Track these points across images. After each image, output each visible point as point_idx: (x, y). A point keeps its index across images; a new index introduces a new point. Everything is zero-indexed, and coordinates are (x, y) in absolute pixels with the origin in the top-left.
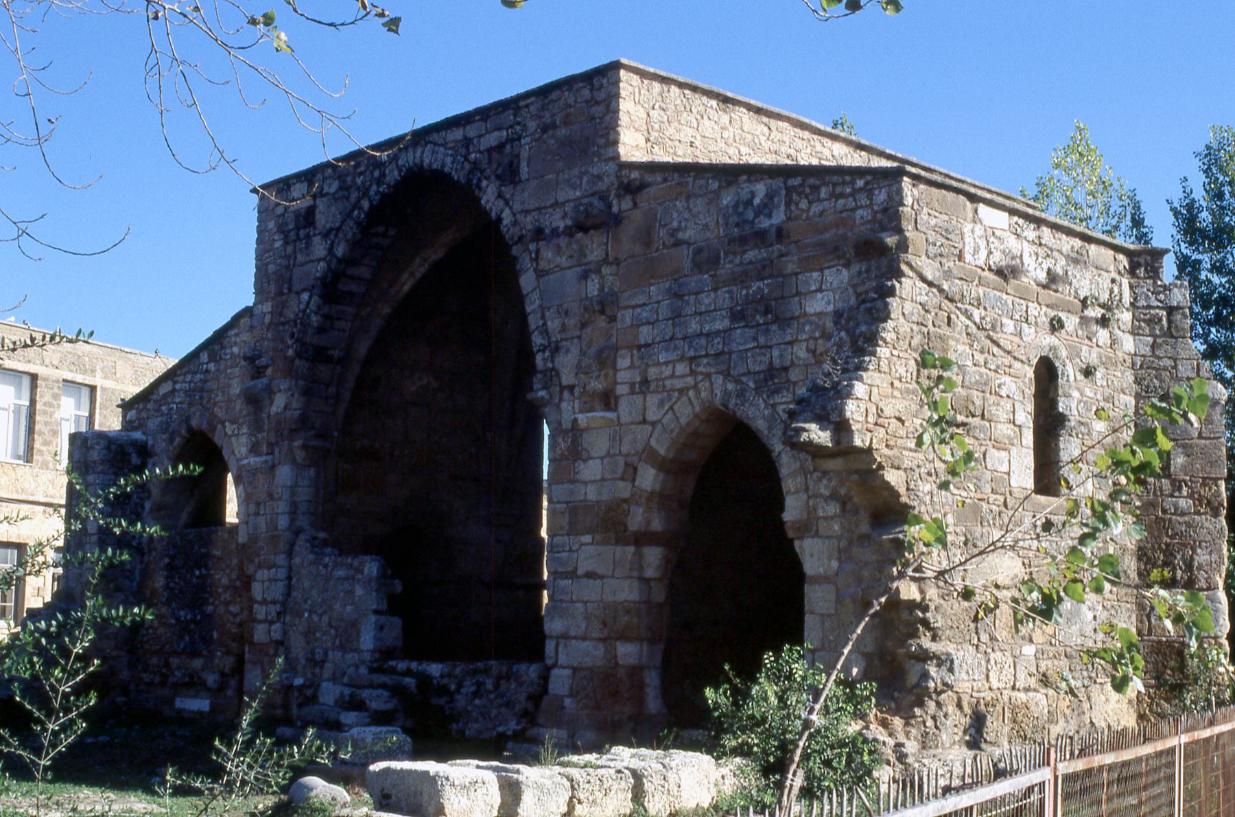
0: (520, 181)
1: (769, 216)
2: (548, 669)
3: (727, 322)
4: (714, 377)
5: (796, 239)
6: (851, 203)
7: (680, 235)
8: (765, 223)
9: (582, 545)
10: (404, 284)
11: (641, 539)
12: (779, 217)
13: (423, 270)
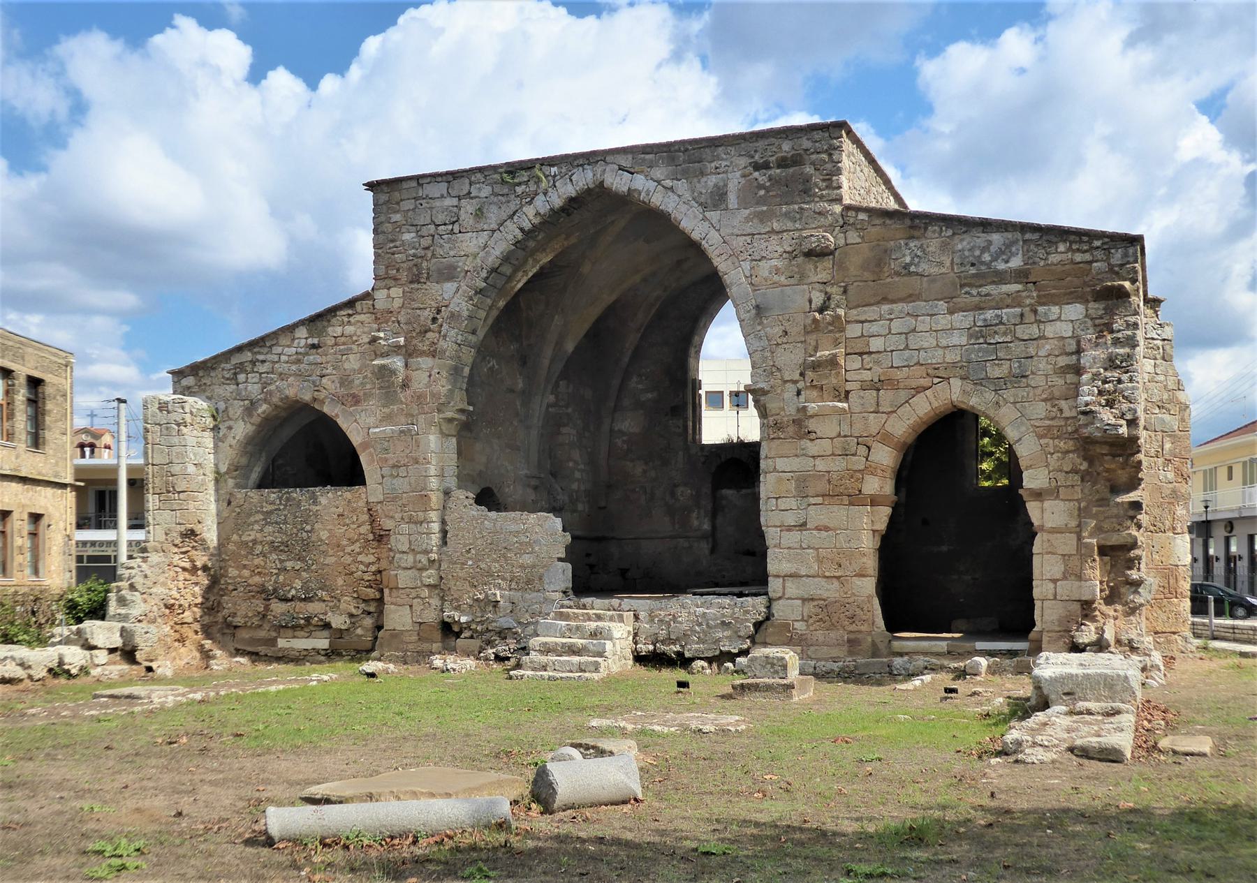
0: (726, 209)
1: (1007, 262)
2: (770, 600)
3: (964, 340)
4: (952, 380)
5: (1034, 280)
6: (1088, 257)
7: (913, 269)
8: (1001, 266)
9: (809, 505)
10: (519, 281)
11: (874, 501)
12: (1016, 262)
13: (534, 270)
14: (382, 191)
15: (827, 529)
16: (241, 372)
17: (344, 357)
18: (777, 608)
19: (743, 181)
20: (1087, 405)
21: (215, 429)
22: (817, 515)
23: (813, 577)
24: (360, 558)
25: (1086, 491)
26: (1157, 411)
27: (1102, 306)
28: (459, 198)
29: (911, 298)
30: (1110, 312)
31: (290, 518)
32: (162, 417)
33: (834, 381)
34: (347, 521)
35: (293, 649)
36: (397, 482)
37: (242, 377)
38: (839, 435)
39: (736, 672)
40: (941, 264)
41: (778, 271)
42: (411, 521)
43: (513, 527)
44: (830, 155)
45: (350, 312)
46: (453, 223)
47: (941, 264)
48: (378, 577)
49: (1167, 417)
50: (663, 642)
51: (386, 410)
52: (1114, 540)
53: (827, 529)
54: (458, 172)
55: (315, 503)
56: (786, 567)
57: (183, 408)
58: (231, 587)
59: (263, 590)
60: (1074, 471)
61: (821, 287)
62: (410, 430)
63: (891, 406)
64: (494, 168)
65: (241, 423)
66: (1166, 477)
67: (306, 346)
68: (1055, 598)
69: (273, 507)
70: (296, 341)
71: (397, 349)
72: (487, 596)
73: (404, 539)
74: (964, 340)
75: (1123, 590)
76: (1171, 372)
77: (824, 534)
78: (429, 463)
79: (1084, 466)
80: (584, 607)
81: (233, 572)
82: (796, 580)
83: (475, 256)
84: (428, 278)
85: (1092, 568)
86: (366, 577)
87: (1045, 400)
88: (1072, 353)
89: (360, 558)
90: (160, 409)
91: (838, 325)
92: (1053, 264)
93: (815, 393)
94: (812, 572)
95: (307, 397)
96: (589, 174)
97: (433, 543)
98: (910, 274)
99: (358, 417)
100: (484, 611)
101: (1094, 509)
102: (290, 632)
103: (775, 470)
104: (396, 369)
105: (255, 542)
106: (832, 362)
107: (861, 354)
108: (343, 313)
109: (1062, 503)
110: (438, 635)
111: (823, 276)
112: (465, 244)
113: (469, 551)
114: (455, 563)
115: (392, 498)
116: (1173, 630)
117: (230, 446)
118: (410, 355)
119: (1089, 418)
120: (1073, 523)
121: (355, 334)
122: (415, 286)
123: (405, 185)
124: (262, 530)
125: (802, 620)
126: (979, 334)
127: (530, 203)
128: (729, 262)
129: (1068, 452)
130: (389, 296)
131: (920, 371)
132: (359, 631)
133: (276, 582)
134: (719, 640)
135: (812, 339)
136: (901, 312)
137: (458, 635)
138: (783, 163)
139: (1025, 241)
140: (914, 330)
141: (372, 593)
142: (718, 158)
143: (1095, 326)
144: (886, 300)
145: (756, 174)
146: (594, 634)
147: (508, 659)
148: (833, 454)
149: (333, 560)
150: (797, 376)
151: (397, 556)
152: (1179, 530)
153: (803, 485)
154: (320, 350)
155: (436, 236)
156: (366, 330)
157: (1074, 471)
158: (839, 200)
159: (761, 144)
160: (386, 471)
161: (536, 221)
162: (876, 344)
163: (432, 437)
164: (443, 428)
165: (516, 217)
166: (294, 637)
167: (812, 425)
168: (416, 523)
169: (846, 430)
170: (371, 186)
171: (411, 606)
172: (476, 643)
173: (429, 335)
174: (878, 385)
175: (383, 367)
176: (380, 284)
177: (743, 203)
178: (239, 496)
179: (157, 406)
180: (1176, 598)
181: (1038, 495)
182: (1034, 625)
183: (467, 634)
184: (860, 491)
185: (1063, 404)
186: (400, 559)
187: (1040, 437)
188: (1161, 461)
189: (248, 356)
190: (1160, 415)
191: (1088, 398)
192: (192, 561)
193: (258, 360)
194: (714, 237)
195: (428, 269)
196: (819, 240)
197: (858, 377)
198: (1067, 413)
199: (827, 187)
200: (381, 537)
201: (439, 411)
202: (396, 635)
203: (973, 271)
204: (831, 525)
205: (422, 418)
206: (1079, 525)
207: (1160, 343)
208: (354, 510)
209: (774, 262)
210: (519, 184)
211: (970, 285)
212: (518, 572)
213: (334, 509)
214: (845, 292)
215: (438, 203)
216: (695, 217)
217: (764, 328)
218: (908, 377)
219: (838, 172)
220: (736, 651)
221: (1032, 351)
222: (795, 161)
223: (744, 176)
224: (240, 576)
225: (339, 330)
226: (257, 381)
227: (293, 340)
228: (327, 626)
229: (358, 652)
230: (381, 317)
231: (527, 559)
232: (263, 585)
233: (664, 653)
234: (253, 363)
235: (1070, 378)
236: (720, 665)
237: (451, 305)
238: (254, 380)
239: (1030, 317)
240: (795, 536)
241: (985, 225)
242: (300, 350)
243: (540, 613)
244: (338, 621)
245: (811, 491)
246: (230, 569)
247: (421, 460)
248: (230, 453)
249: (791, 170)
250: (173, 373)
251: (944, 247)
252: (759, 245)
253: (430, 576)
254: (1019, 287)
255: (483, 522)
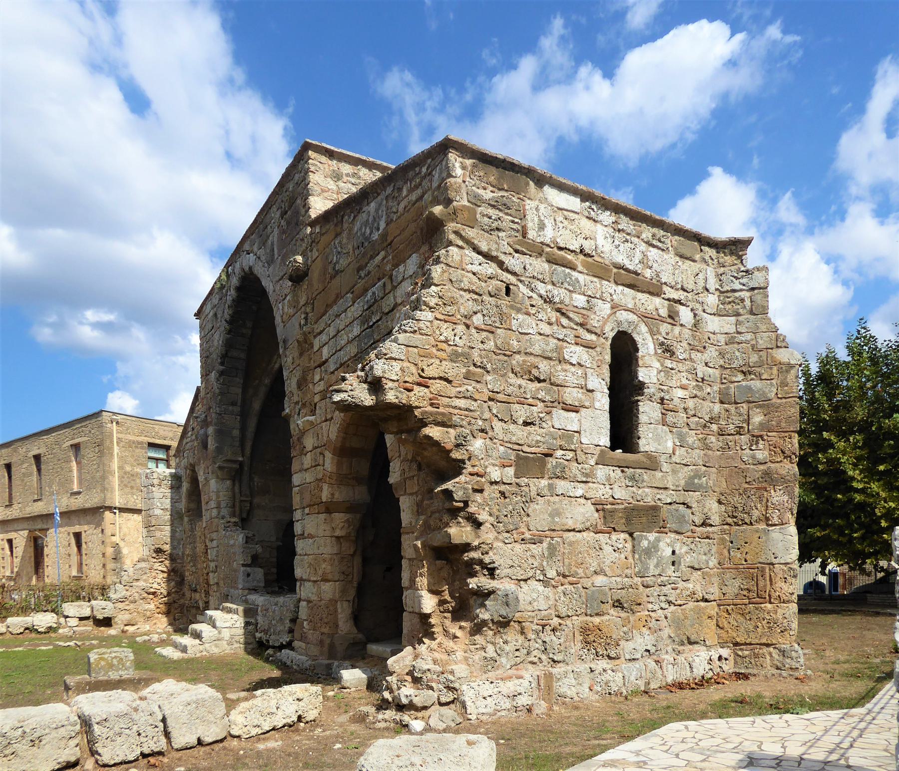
1: (378, 229)
26: (740, 377)
49: (756, 384)
66: (753, 457)
76: (763, 327)
116: (764, 641)
152: (776, 520)
180: (770, 603)
188: (744, 439)
190: (744, 383)
207: (746, 295)
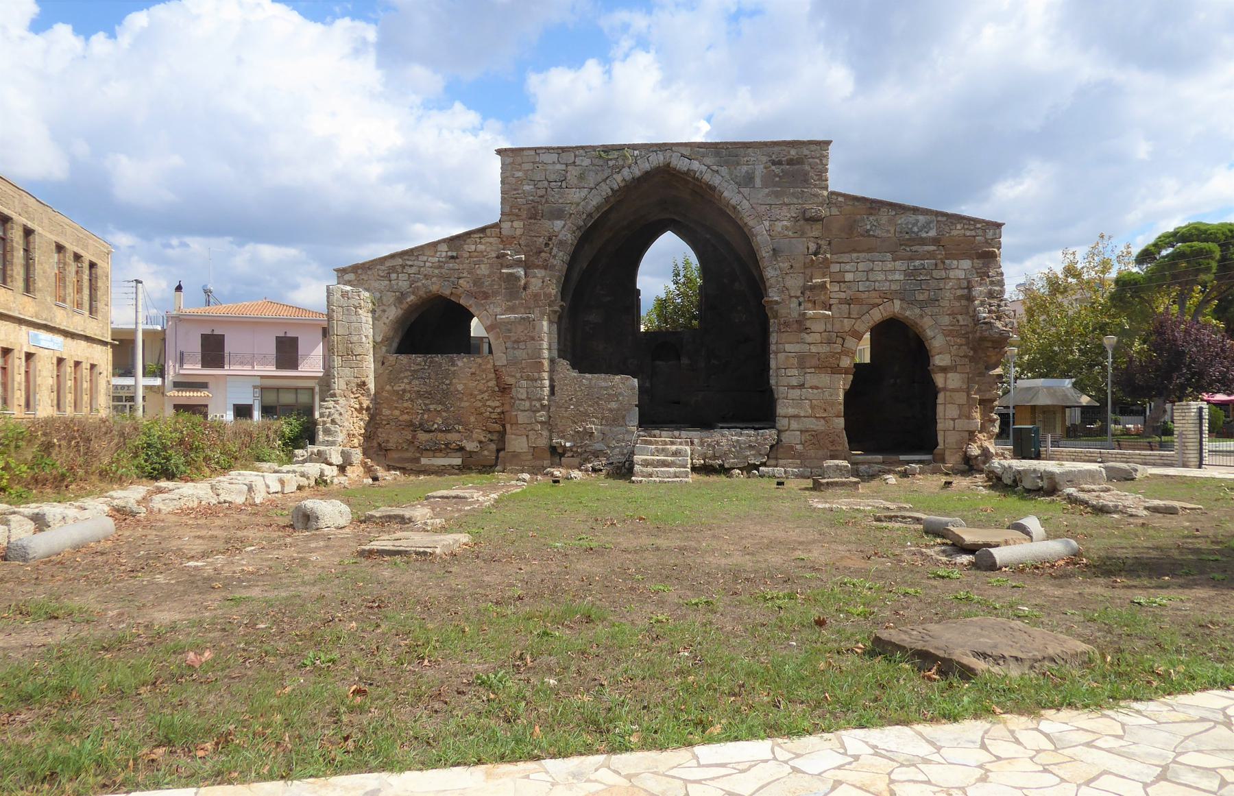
0: (754, 187)
3: (902, 277)
6: (973, 233)
7: (871, 233)
8: (924, 235)
12: (932, 233)
14: (508, 156)
15: (817, 388)
16: (393, 273)
17: (477, 266)
18: (786, 437)
19: (765, 171)
20: (985, 318)
21: (373, 312)
22: (811, 380)
23: (808, 417)
24: (488, 403)
25: (972, 368)
27: (981, 262)
28: (567, 165)
29: (870, 250)
30: (987, 265)
31: (433, 374)
32: (344, 302)
33: (823, 298)
34: (478, 378)
35: (433, 465)
36: (518, 353)
37: (394, 276)
38: (825, 331)
39: (760, 476)
40: (888, 231)
41: (787, 228)
42: (528, 379)
43: (604, 384)
44: (821, 160)
45: (482, 235)
46: (562, 181)
47: (888, 231)
48: (502, 416)
50: (710, 459)
51: (509, 303)
52: (987, 396)
53: (817, 388)
54: (567, 148)
55: (453, 365)
56: (791, 411)
57: (359, 296)
58: (384, 422)
59: (411, 424)
60: (965, 356)
61: (815, 240)
62: (528, 317)
63: (858, 314)
64: (594, 148)
65: (393, 308)
67: (446, 257)
68: (954, 429)
69: (419, 367)
70: (439, 253)
71: (518, 263)
72: (585, 428)
73: (523, 391)
74: (902, 277)
75: (987, 425)
77: (815, 391)
78: (543, 340)
79: (971, 353)
80: (655, 436)
81: (386, 412)
82: (797, 419)
83: (578, 204)
84: (542, 217)
85: (976, 412)
86: (493, 417)
87: (949, 315)
88: (964, 288)
89: (488, 403)
90: (342, 296)
91: (826, 263)
92: (953, 236)
93: (810, 305)
94: (808, 414)
95: (447, 292)
96: (661, 158)
97: (545, 394)
98: (870, 236)
99: (487, 307)
100: (582, 439)
101: (977, 379)
102: (431, 453)
103: (785, 351)
104: (520, 277)
105: (404, 391)
106: (823, 286)
107: (838, 282)
108: (476, 236)
109: (958, 375)
110: (548, 455)
111: (816, 234)
112: (570, 196)
113: (571, 400)
114: (561, 407)
115: (513, 362)
117: (384, 324)
118: (528, 268)
119: (989, 326)
120: (965, 387)
121: (486, 251)
122: (533, 221)
123: (525, 153)
124: (410, 383)
125: (801, 443)
126: (910, 274)
127: (618, 173)
128: (755, 221)
129: (961, 345)
130: (512, 227)
131: (874, 294)
132: (486, 453)
133: (421, 419)
134: (748, 456)
135: (808, 271)
136: (864, 258)
137: (562, 455)
138: (791, 162)
139: (938, 221)
140: (872, 270)
141: (497, 427)
142: (749, 155)
143: (977, 273)
144: (855, 251)
145: (773, 167)
146: (675, 454)
147: (601, 470)
148: (821, 343)
149: (467, 404)
150: (799, 294)
151: (517, 402)
153: (802, 362)
154: (457, 261)
155: (549, 189)
156: (494, 248)
157: (965, 356)
158: (826, 188)
159: (776, 149)
160: (509, 344)
161: (622, 184)
162: (849, 277)
163: (545, 323)
164: (551, 317)
165: (608, 181)
166: (434, 457)
167: (808, 324)
168: (532, 380)
169: (829, 327)
170: (499, 152)
171: (527, 436)
172: (576, 461)
173: (543, 255)
174: (850, 302)
175: (511, 274)
176: (505, 218)
177: (765, 185)
178: (391, 359)
179: (340, 293)
181: (944, 370)
182: (937, 444)
183: (570, 454)
184: (838, 365)
185: (960, 317)
186: (520, 404)
187: (946, 336)
189: (400, 261)
191: (984, 315)
192: (361, 404)
193: (407, 265)
194: (746, 204)
195: (542, 210)
196: (816, 212)
197: (838, 296)
198: (961, 323)
199: (818, 180)
200: (504, 390)
201: (549, 306)
202: (516, 455)
203: (907, 236)
204: (820, 386)
205: (537, 311)
206: (968, 388)
208: (484, 371)
209: (785, 223)
210: (611, 160)
211: (906, 245)
212: (607, 414)
213: (467, 370)
214: (829, 244)
215: (550, 167)
216: (733, 191)
217: (778, 262)
218: (868, 298)
219: (826, 171)
220: (758, 463)
221: (942, 285)
222: (799, 161)
223: (765, 168)
224: (392, 414)
225: (473, 247)
226: (406, 279)
227: (436, 252)
228: (462, 449)
229: (484, 466)
230: (505, 241)
231: (614, 405)
232: (411, 421)
233: (711, 466)
234: (403, 267)
235: (964, 302)
236: (749, 472)
237: (560, 236)
238: (404, 279)
239: (940, 266)
240: (797, 392)
241: (916, 210)
242: (441, 259)
243: (623, 440)
244: (470, 446)
245: (808, 365)
246: (384, 410)
247: (536, 338)
248: (385, 328)
249: (796, 167)
250: (337, 270)
251: (890, 221)
252: (775, 211)
253: (542, 416)
254: (935, 248)
255: (581, 381)
